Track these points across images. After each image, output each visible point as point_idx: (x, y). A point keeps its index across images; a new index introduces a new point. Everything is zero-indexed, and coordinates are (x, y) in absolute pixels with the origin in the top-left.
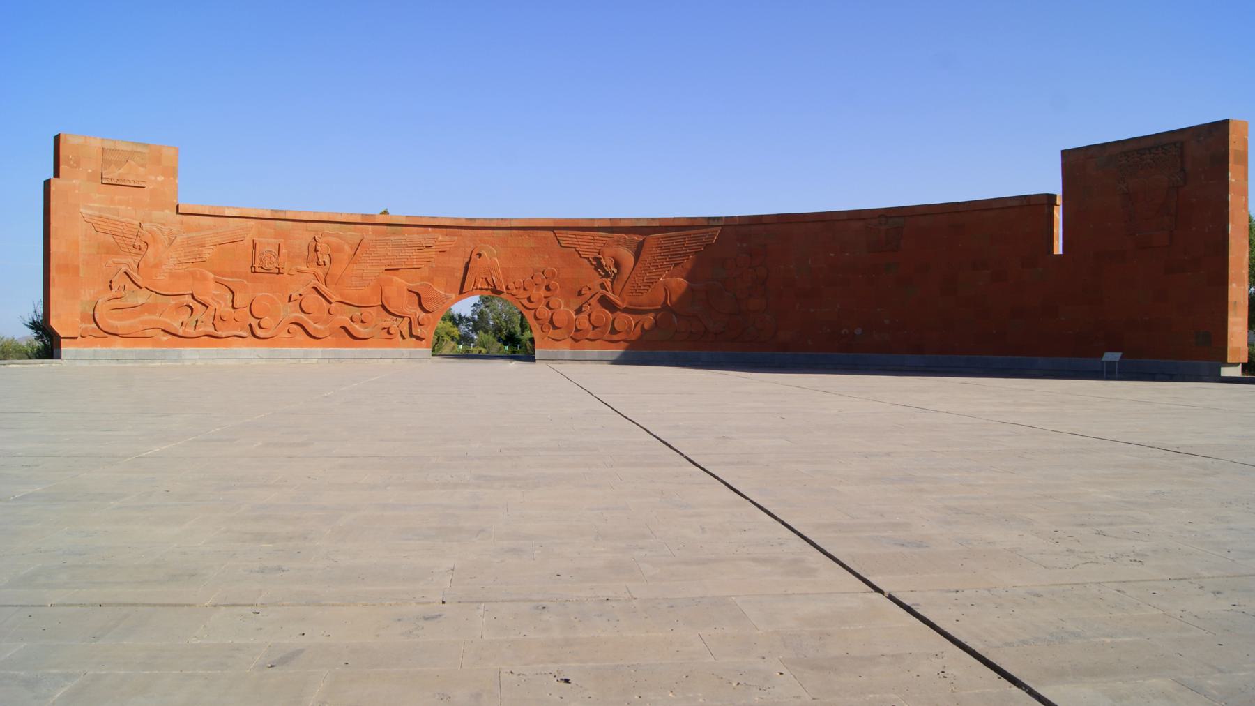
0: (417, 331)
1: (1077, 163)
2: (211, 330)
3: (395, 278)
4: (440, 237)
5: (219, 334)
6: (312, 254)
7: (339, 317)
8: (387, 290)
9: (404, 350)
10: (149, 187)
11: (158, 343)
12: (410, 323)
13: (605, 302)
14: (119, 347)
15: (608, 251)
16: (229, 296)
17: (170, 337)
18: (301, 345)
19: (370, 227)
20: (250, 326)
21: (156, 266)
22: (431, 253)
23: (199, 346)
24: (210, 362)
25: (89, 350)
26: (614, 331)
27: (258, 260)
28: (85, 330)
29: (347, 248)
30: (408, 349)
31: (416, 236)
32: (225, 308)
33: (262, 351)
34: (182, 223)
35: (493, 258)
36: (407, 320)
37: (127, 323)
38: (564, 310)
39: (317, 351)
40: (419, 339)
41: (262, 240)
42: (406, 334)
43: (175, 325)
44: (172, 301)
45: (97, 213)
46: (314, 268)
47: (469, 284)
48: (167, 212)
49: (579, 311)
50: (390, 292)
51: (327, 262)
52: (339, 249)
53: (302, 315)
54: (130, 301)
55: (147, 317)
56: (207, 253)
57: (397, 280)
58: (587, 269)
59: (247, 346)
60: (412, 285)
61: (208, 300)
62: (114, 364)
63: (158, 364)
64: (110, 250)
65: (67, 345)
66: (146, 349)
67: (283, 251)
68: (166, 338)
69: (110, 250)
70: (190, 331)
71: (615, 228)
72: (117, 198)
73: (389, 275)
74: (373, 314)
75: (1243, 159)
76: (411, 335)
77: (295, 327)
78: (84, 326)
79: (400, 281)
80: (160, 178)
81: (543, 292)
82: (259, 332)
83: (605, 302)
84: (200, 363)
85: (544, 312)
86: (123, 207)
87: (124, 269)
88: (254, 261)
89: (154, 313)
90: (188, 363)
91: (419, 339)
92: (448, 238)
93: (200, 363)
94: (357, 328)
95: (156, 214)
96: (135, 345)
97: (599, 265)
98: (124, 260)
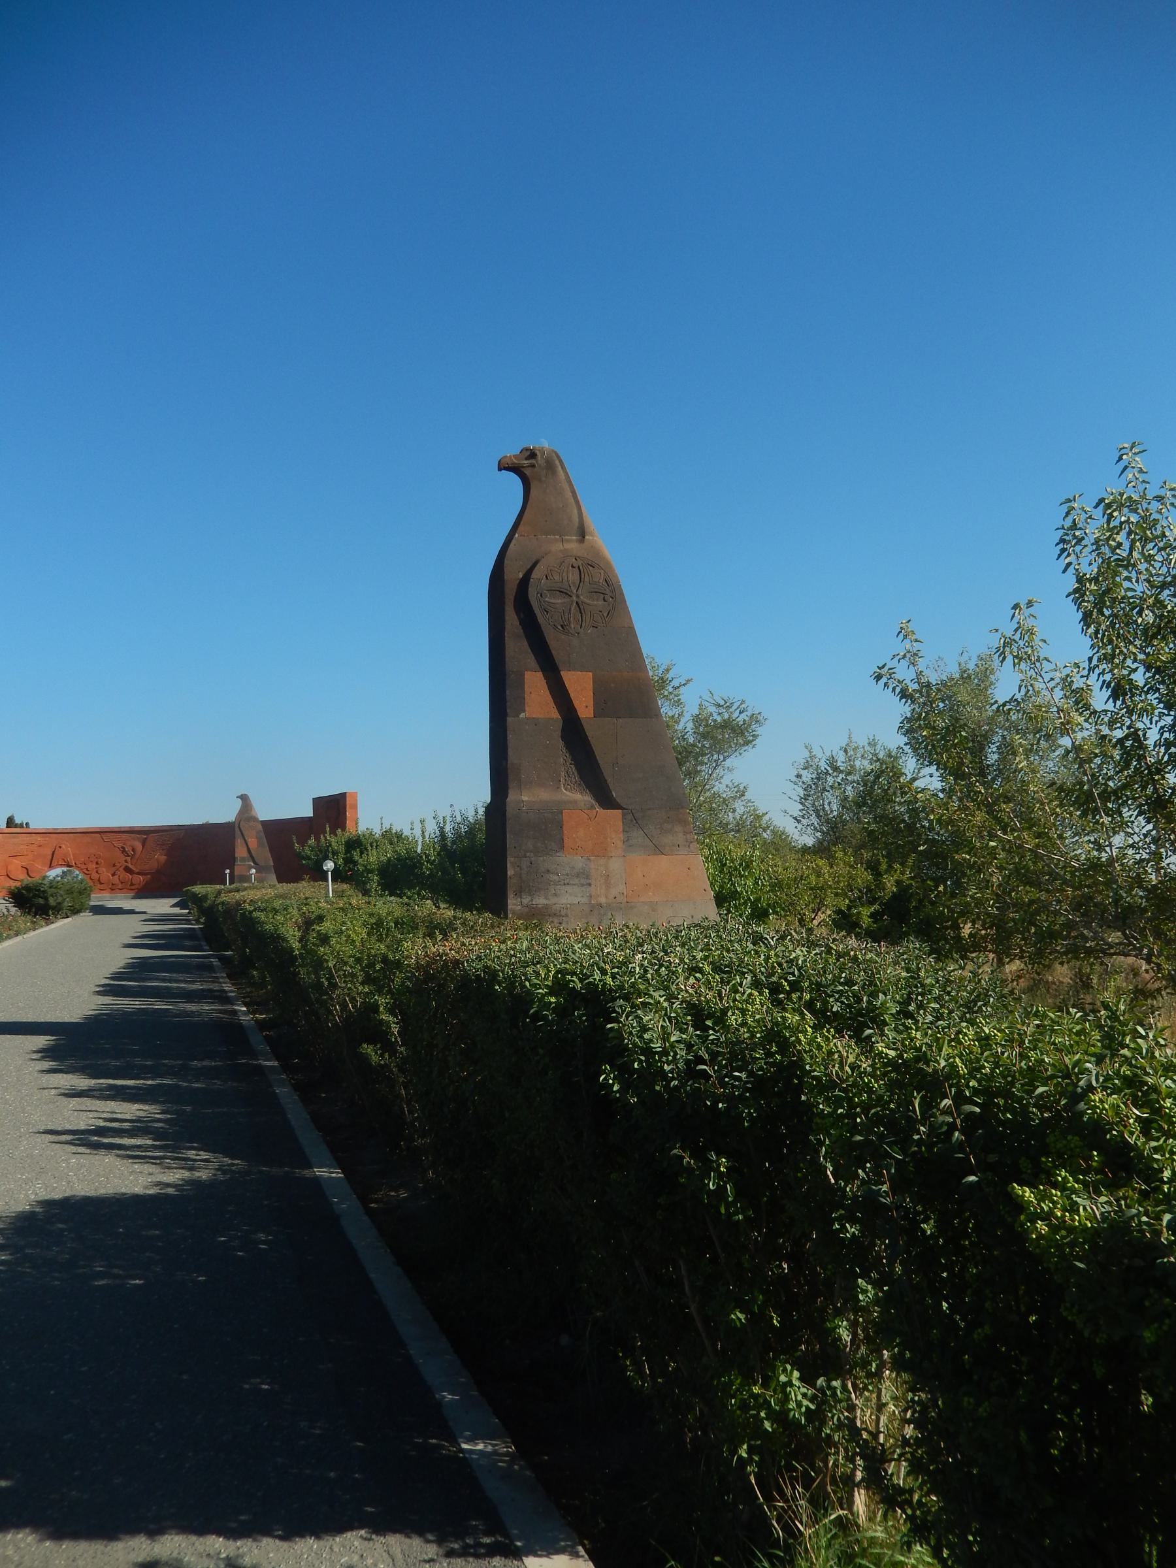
1: (318, 803)
4: (39, 838)
13: (127, 870)
15: (129, 843)
22: (34, 847)
26: (132, 884)
35: (68, 849)
38: (106, 874)
47: (55, 862)
49: (113, 875)
57: (15, 861)
58: (118, 853)
71: (132, 831)
75: (355, 807)
81: (94, 866)
83: (127, 870)
85: (95, 876)
97: (124, 851)
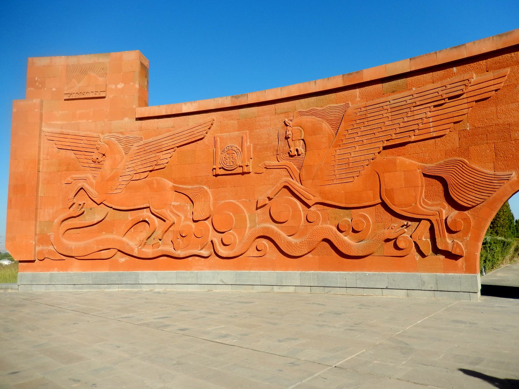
0: (446, 242)
2: (169, 249)
3: (400, 159)
4: (474, 75)
5: (180, 253)
6: (283, 143)
7: (321, 225)
8: (387, 178)
9: (425, 276)
10: (110, 96)
11: (116, 266)
12: (432, 230)
14: (76, 271)
16: (189, 206)
17: (128, 258)
18: (273, 266)
19: (357, 91)
20: (212, 241)
21: (112, 179)
22: (461, 106)
23: (157, 268)
24: (169, 288)
25: (45, 274)
27: (218, 160)
28: (40, 252)
29: (326, 126)
30: (432, 275)
31: (431, 86)
32: (184, 222)
33: (227, 274)
34: (141, 129)
36: (425, 226)
37: (82, 244)
39: (293, 277)
40: (450, 255)
41: (225, 134)
42: (427, 248)
43: (132, 243)
44: (130, 217)
45: (59, 130)
46: (285, 162)
48: (126, 119)
50: (393, 181)
51: (301, 150)
52: (315, 130)
53: (274, 226)
54: (88, 219)
55: (105, 236)
56: (164, 158)
59: (210, 267)
60: (431, 167)
61: (166, 213)
62: (70, 289)
63: (115, 289)
64: (69, 167)
65: (24, 269)
66: (102, 272)
67: (247, 143)
68: (123, 259)
69: (69, 167)
70: (149, 251)
72: (78, 112)
73: (388, 155)
74: (370, 217)
76: (436, 250)
77: (265, 242)
78: (38, 249)
79: (407, 162)
80: (120, 86)
82: (223, 251)
84: (158, 289)
86: (84, 121)
87: (80, 185)
88: (214, 163)
89: (111, 232)
90: (145, 289)
91: (450, 255)
92: (490, 75)
93: (158, 289)
94: (348, 242)
95: (116, 124)
96: (93, 268)
98: (83, 176)
